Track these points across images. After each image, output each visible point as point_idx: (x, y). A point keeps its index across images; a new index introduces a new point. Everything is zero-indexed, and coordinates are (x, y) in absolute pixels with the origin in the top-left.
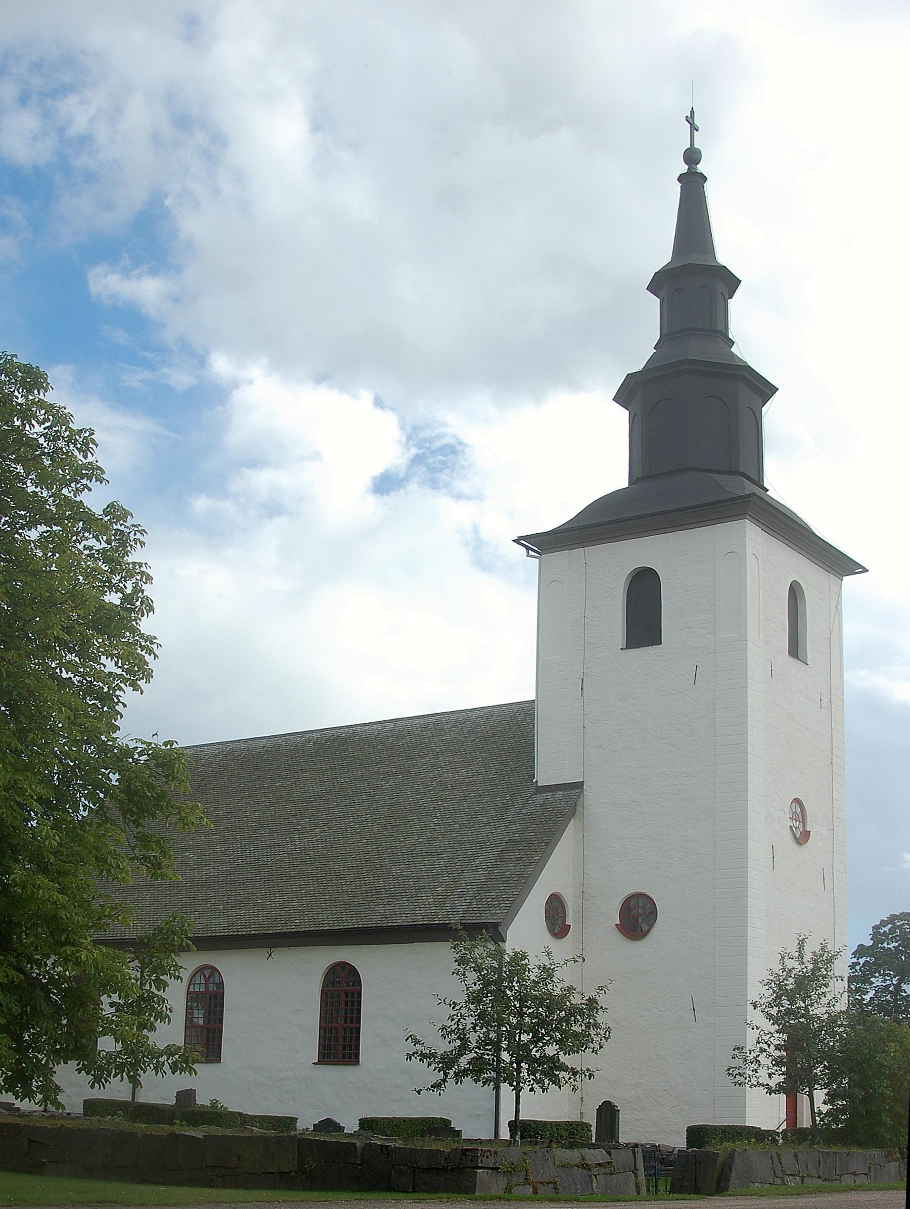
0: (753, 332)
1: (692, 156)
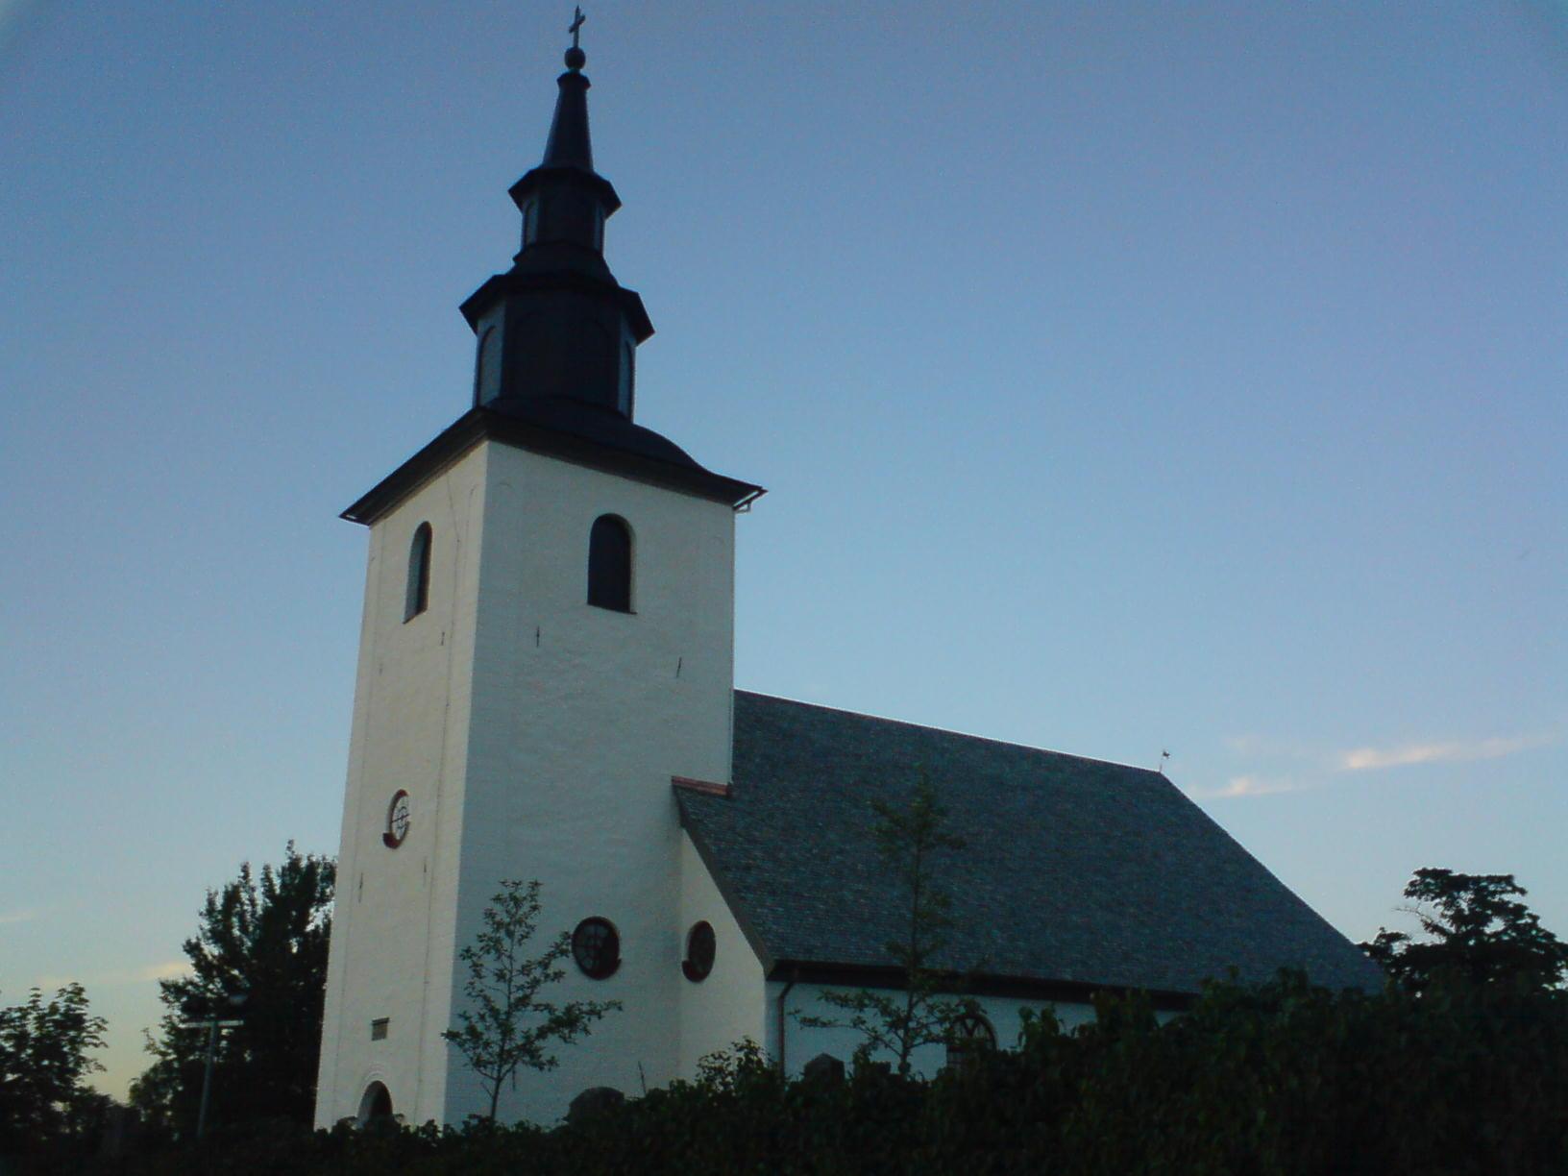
1: (575, 58)
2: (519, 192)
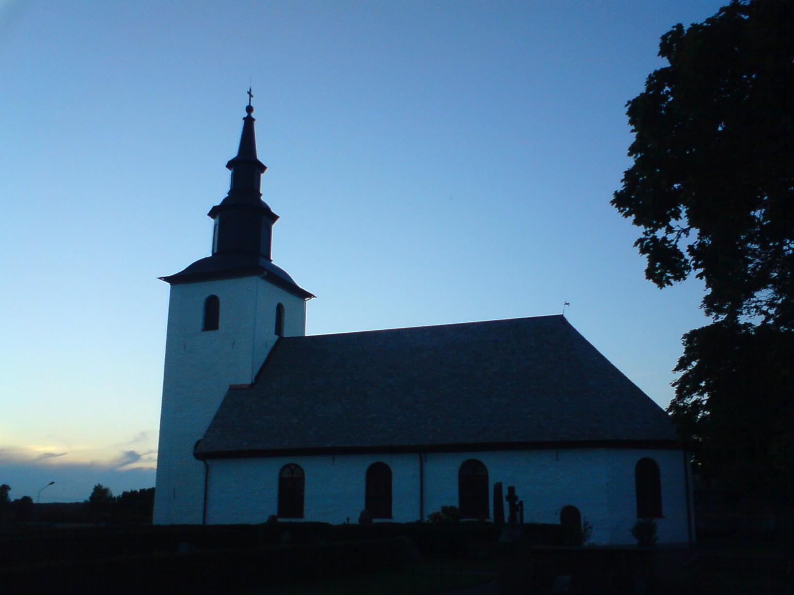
0: (270, 191)
1: (249, 109)
2: (230, 165)
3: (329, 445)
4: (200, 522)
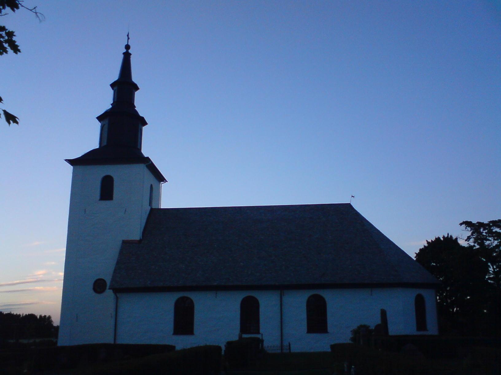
1: (128, 47)
2: (113, 85)
3: (215, 284)
4: (112, 342)
